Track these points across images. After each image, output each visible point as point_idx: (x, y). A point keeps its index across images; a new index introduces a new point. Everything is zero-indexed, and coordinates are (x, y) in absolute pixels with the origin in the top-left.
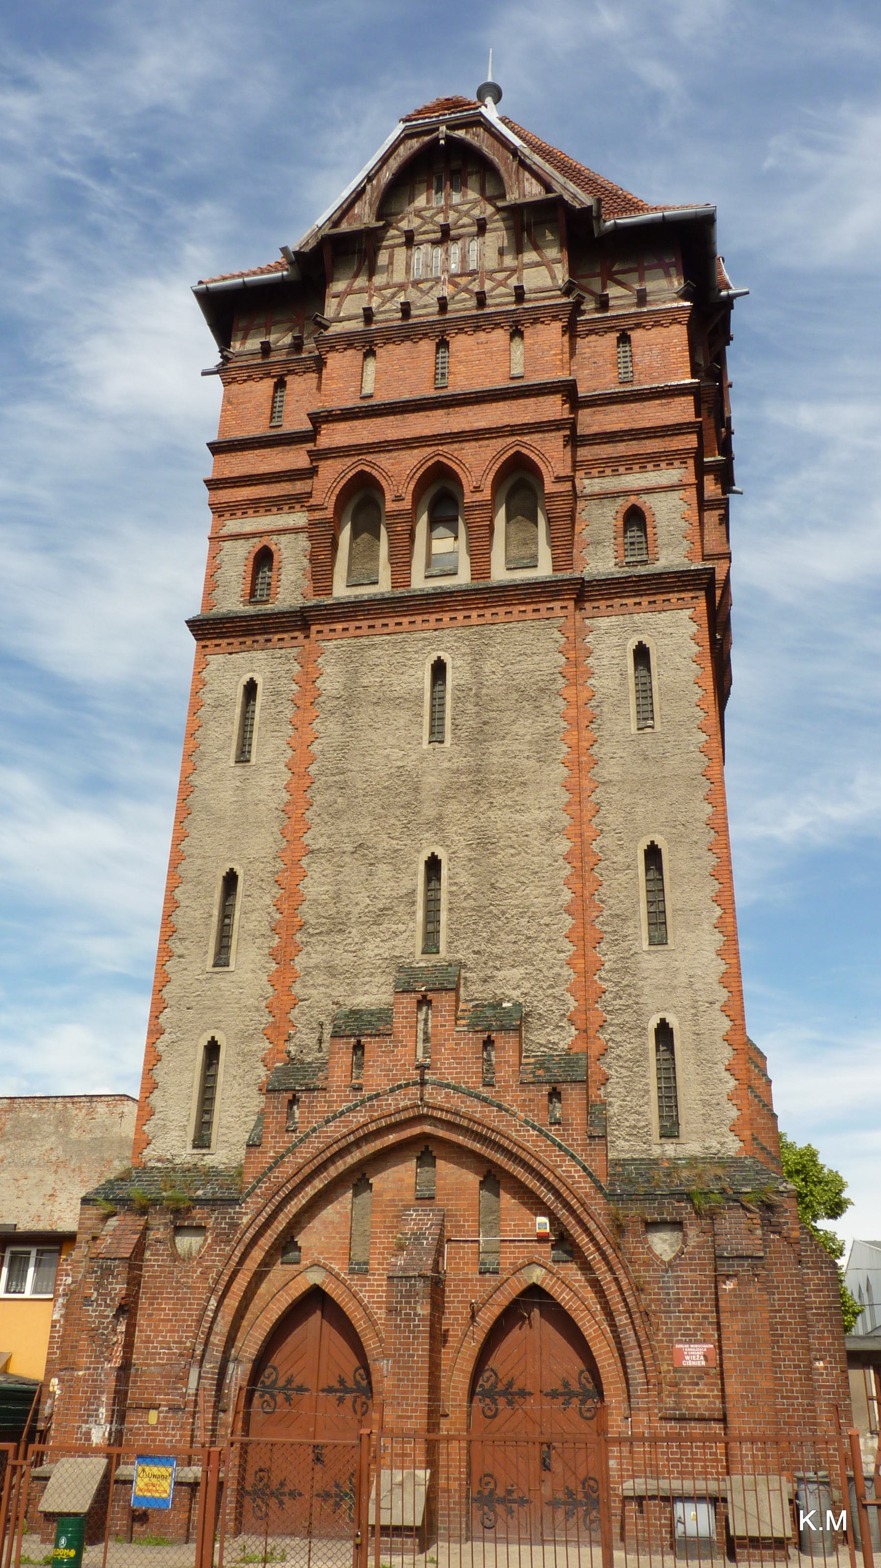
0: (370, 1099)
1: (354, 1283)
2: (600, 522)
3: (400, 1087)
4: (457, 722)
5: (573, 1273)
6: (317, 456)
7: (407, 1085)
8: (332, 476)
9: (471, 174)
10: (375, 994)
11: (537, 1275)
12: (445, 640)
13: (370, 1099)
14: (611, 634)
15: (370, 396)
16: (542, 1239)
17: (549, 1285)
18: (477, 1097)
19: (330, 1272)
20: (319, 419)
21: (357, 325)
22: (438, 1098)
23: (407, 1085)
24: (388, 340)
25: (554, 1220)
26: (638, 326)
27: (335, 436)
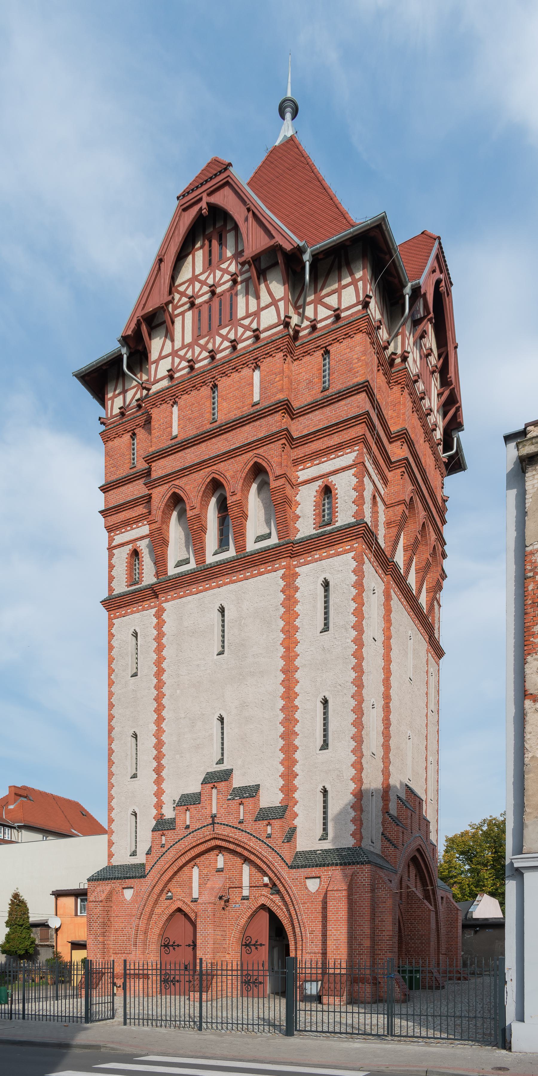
0: (193, 832)
1: (192, 905)
2: (306, 500)
3: (204, 826)
4: (230, 642)
5: (277, 898)
6: (152, 485)
7: (208, 825)
8: (160, 495)
9: (230, 231)
10: (194, 787)
11: (262, 901)
12: (224, 593)
13: (193, 832)
14: (309, 575)
15: (176, 437)
16: (266, 885)
17: (268, 903)
18: (236, 828)
19: (184, 902)
20: (151, 459)
21: (165, 383)
22: (220, 830)
23: (208, 825)
24: (186, 392)
25: (270, 879)
26: (337, 340)
27: (161, 468)
